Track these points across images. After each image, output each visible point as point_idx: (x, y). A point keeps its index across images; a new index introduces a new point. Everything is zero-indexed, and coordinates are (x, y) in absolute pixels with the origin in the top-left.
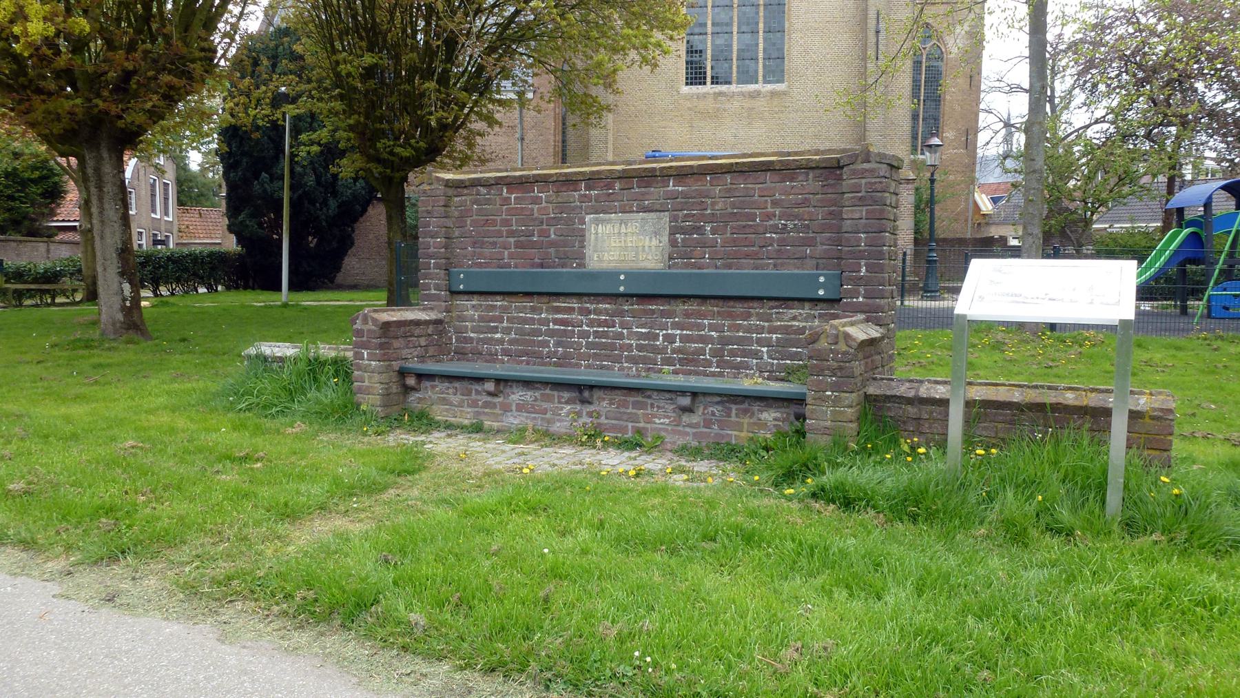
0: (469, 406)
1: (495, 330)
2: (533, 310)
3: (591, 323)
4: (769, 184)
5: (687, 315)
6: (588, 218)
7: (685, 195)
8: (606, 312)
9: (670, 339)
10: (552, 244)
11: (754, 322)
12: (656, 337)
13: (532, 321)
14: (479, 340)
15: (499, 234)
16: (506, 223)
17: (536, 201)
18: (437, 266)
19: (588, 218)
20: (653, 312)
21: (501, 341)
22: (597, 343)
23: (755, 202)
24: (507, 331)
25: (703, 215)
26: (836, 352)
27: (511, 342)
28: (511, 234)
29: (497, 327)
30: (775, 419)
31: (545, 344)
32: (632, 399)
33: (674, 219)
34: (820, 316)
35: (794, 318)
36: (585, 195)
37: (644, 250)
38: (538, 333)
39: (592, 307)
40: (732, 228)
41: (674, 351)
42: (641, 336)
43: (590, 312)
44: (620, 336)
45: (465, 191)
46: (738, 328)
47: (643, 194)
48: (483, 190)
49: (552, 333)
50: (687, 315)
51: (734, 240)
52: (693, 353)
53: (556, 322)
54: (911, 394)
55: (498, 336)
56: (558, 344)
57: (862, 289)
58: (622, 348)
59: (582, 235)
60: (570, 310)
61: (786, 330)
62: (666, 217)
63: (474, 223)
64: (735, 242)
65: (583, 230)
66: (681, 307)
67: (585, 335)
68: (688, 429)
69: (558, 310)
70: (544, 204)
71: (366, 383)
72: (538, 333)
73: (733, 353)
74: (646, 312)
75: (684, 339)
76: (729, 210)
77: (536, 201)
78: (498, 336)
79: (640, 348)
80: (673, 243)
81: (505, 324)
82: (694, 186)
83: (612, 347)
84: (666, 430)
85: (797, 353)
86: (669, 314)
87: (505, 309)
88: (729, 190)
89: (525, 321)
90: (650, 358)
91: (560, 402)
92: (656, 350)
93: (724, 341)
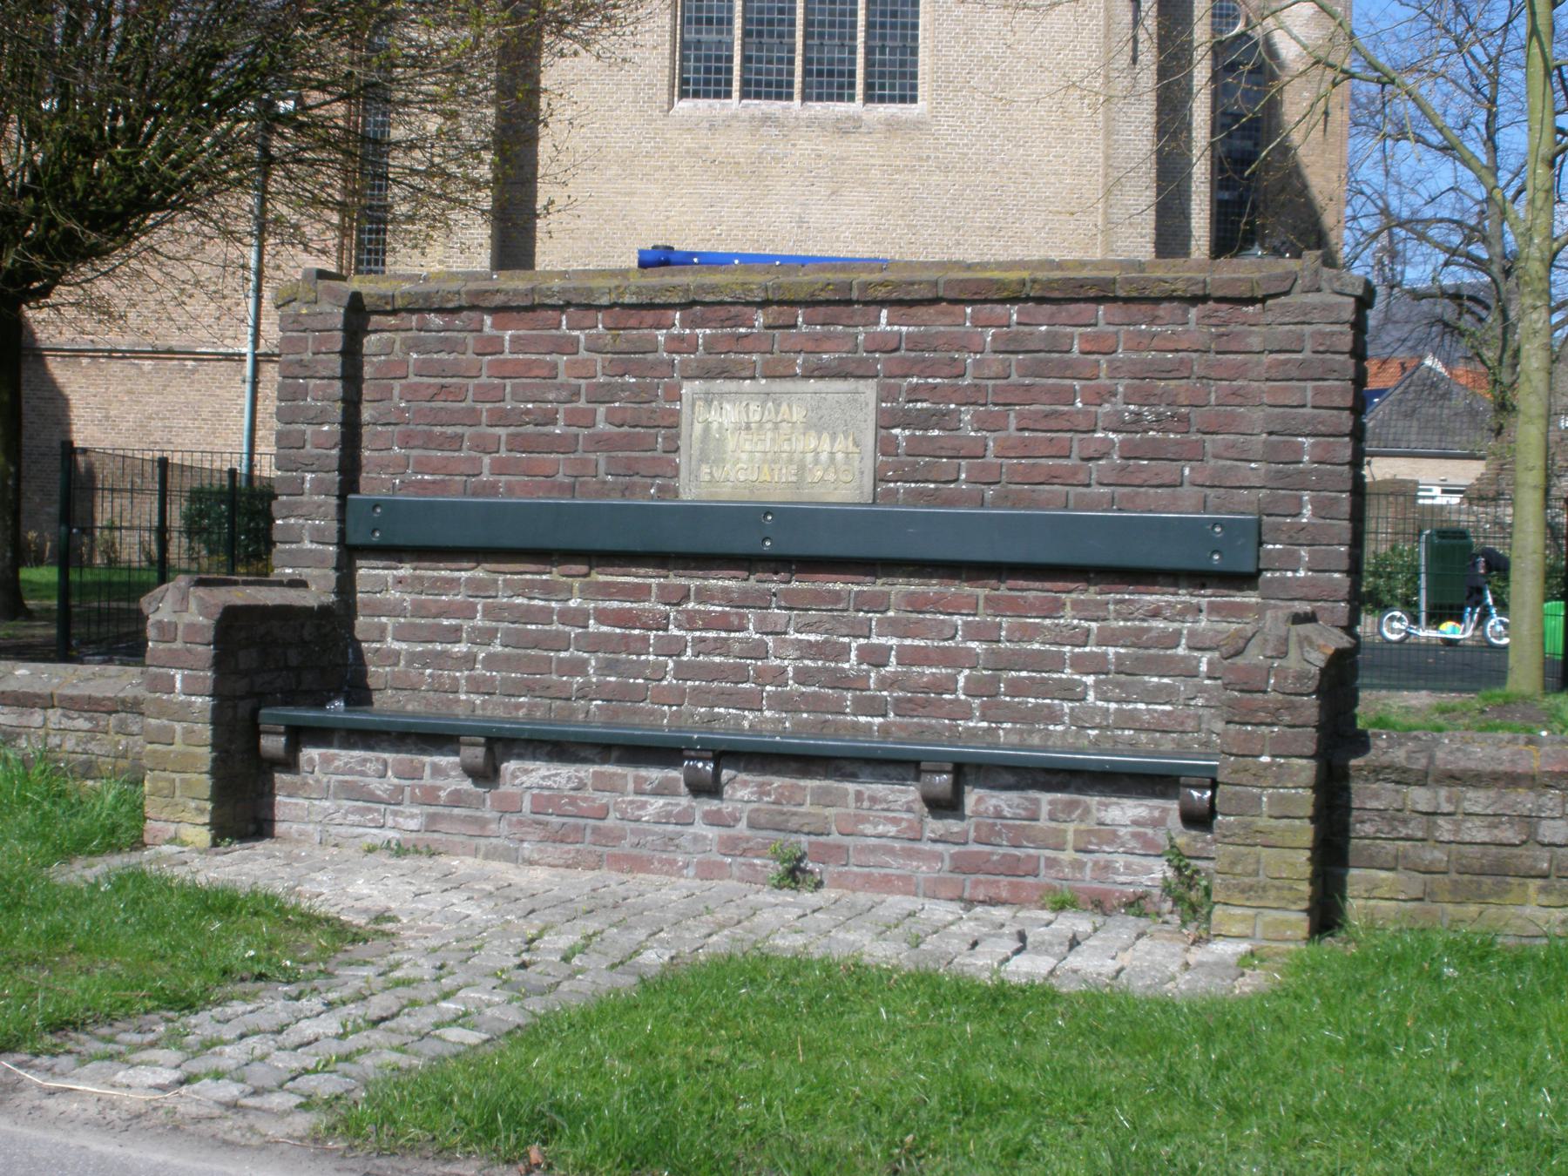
0: (415, 801)
1: (454, 635)
2: (548, 590)
3: (690, 622)
4: (1102, 326)
5: (917, 604)
6: (688, 388)
7: (915, 344)
8: (726, 596)
9: (876, 657)
10: (601, 443)
11: (1069, 619)
12: (844, 651)
13: (544, 616)
14: (413, 657)
15: (472, 418)
16: (491, 394)
17: (568, 346)
18: (319, 488)
19: (688, 388)
20: (836, 596)
21: (469, 660)
22: (702, 666)
23: (1068, 365)
24: (486, 636)
25: (956, 389)
26: (1281, 673)
27: (491, 662)
28: (500, 419)
29: (458, 629)
30: (1135, 823)
31: (579, 667)
32: (815, 783)
33: (885, 394)
34: (1214, 609)
35: (1155, 614)
36: (680, 338)
37: (816, 462)
38: (561, 642)
39: (694, 584)
40: (1020, 416)
41: (884, 683)
42: (808, 650)
43: (686, 597)
44: (759, 651)
45: (392, 321)
46: (1030, 633)
47: (817, 339)
48: (435, 320)
49: (595, 644)
50: (917, 604)
51: (1025, 443)
52: (926, 689)
53: (603, 617)
54: (1421, 763)
55: (461, 648)
56: (607, 667)
57: (1304, 553)
58: (762, 677)
59: (673, 424)
60: (640, 593)
61: (1135, 639)
62: (868, 391)
63: (411, 393)
64: (1025, 451)
65: (677, 413)
66: (900, 587)
67: (673, 648)
68: (940, 847)
69: (607, 591)
70: (583, 354)
71: (178, 746)
72: (561, 642)
73: (1016, 688)
74: (818, 598)
75: (910, 657)
76: (1014, 378)
77: (568, 346)
78: (461, 648)
79: (803, 676)
80: (885, 446)
81: (479, 621)
82: (937, 323)
83: (740, 674)
84: (891, 851)
85: (1160, 687)
86: (878, 604)
87: (478, 588)
88: (1014, 338)
89: (528, 615)
90: (825, 698)
91: (639, 792)
92: (841, 682)
93: (1001, 663)
